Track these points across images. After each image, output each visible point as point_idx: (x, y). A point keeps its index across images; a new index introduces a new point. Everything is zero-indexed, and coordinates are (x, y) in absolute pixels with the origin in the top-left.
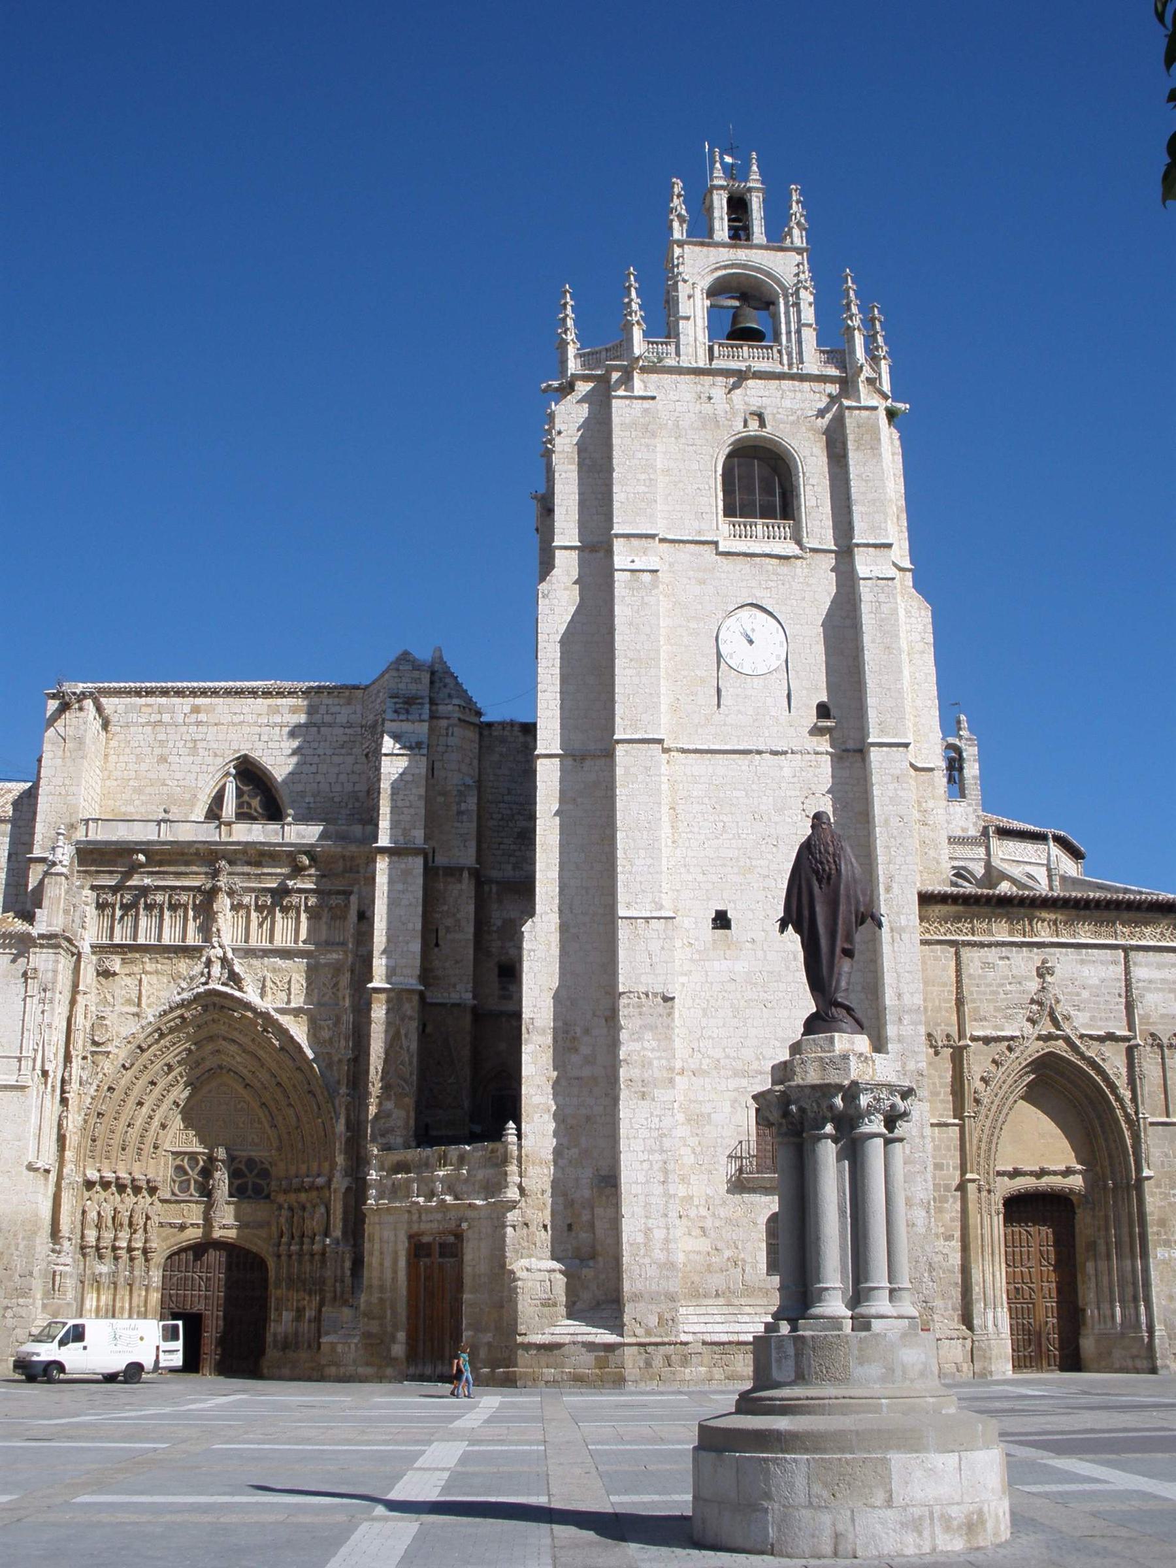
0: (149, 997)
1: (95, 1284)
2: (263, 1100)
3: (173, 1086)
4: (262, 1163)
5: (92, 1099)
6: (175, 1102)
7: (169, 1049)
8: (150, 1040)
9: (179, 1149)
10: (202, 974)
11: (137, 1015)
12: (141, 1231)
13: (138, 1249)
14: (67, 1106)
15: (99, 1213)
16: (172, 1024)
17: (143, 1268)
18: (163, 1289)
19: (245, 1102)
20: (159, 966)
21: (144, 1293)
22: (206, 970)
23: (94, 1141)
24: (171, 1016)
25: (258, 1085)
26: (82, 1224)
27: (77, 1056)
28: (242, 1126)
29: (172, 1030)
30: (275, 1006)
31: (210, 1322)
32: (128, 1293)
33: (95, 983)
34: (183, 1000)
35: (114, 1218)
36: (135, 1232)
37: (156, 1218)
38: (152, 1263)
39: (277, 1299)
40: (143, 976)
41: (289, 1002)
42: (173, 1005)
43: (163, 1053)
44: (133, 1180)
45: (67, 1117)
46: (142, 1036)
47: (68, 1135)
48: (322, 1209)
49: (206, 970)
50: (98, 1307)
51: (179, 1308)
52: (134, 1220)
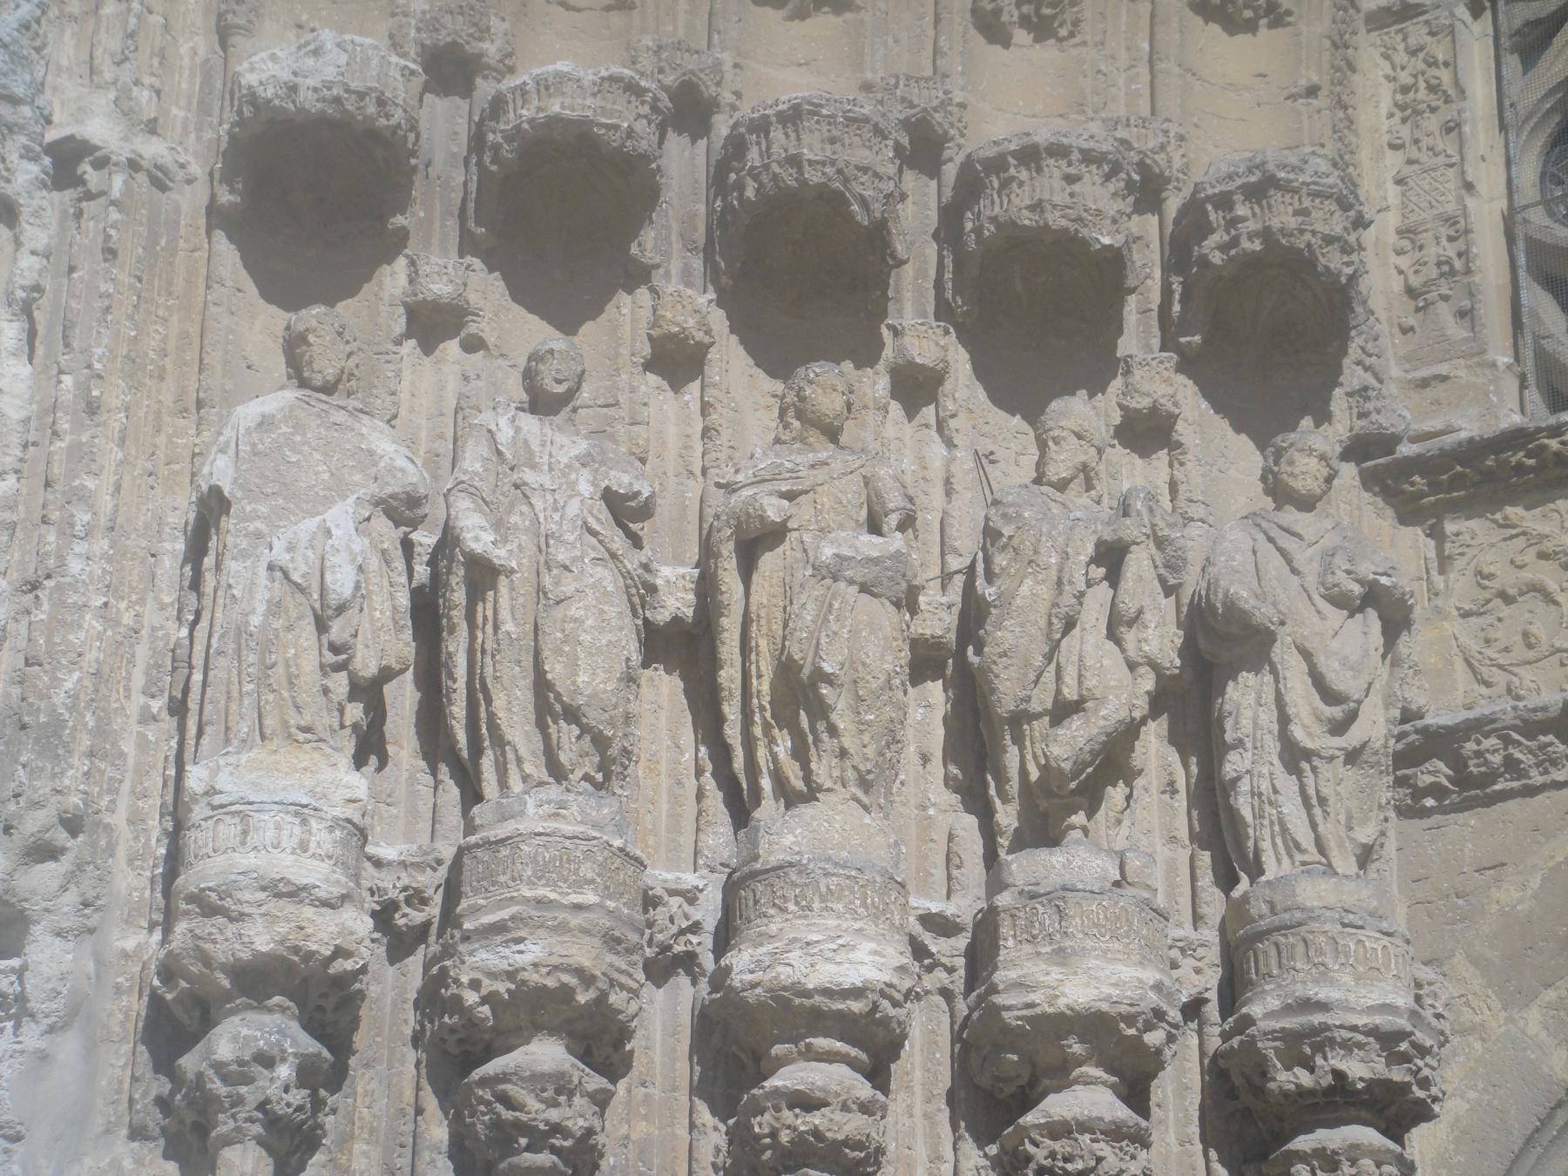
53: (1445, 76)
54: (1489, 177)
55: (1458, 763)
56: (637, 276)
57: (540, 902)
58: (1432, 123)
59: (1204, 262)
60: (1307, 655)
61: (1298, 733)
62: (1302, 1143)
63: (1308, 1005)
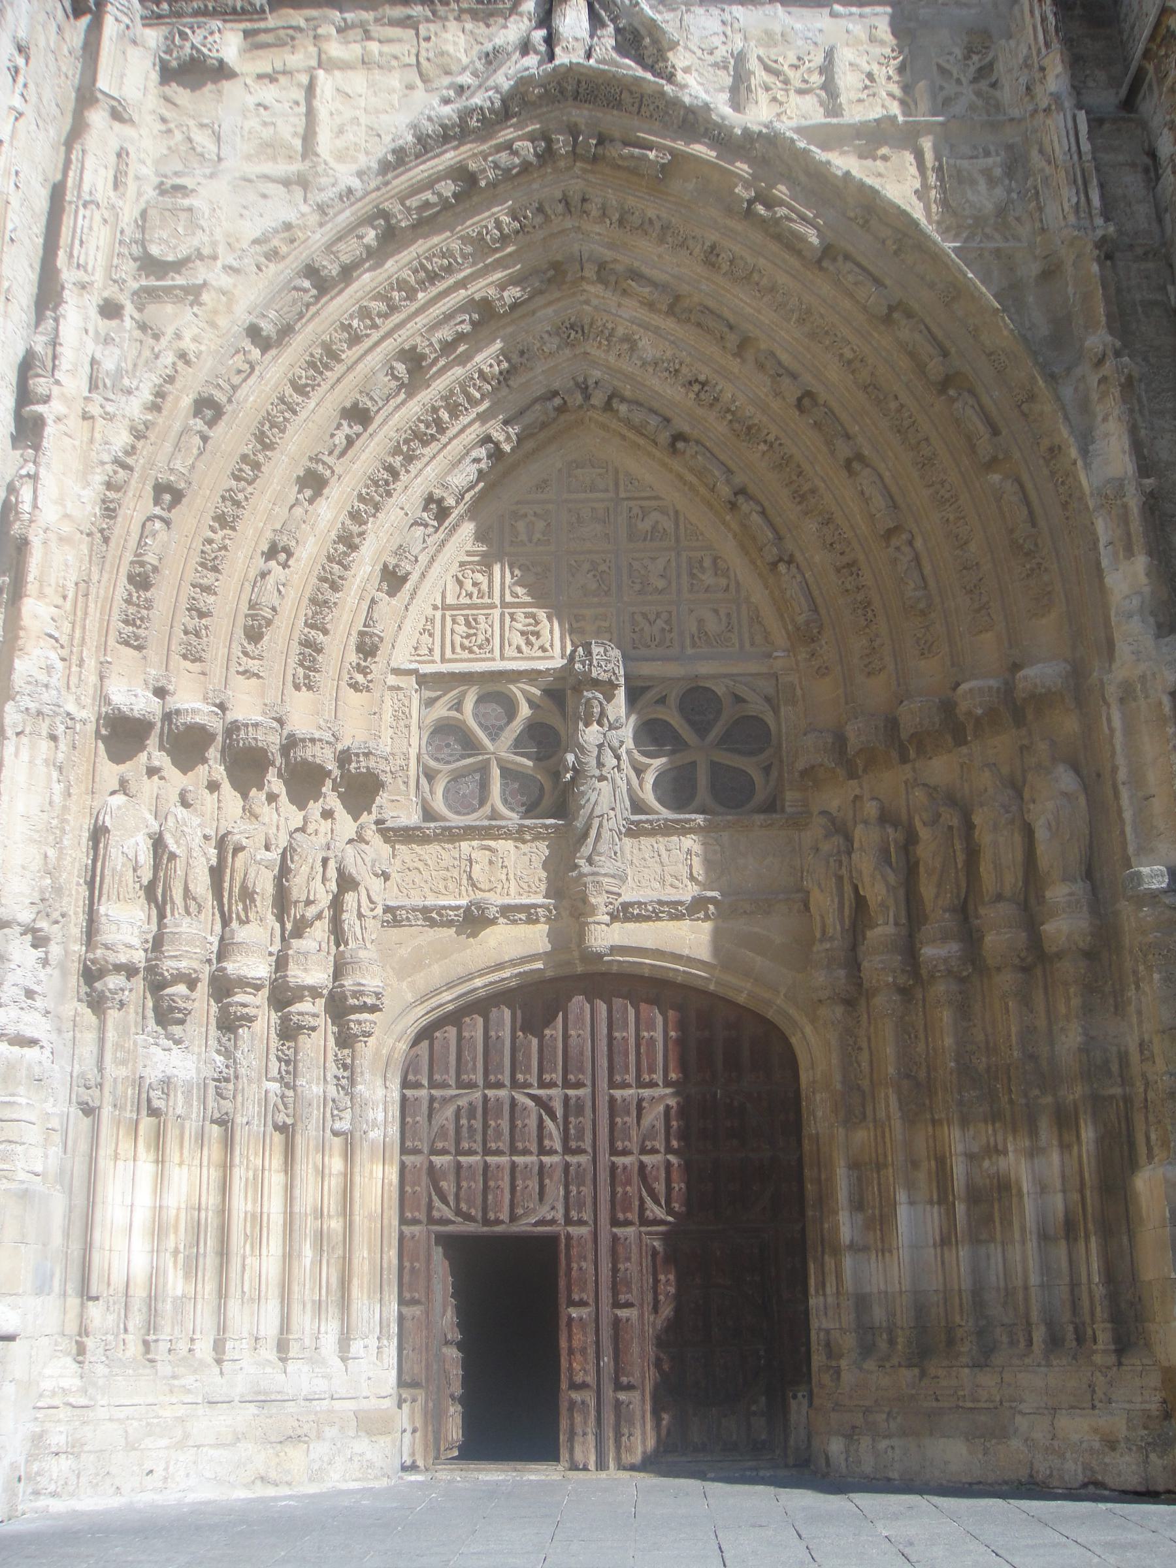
0: (341, 132)
1: (146, 1123)
2: (739, 479)
3: (425, 441)
4: (739, 699)
5: (139, 435)
6: (430, 499)
7: (411, 296)
8: (349, 250)
9: (445, 668)
10: (525, 47)
11: (303, 182)
12: (320, 932)
13: (314, 992)
14: (37, 447)
15: (158, 843)
16: (428, 196)
17: (332, 1069)
18: (404, 1150)
19: (663, 511)
20: (374, 46)
21: (336, 1164)
22: (541, 33)
23: (141, 581)
24: (421, 171)
25: (722, 428)
26: (91, 884)
27: (83, 286)
28: (661, 584)
29: (425, 224)
30: (793, 124)
31: (587, 1265)
32: (277, 1161)
33: (152, 101)
34: (465, 114)
35: (217, 874)
36: (298, 933)
37: (376, 884)
38: (367, 1051)
39: (854, 1165)
40: (321, 73)
41: (833, 109)
42: (430, 128)
43: (393, 308)
44: (291, 743)
45: (34, 478)
46: (319, 238)
47: (36, 542)
48: (1066, 780)
49: (539, 35)
50: (158, 1210)
51: (468, 1217)
52: (297, 887)
53: (407, 710)
54: (415, 741)
55: (395, 916)
56: (204, 761)
57: (187, 951)
58: (402, 723)
59: (349, 771)
60: (367, 890)
61: (362, 910)
62: (352, 1017)
63: (360, 984)
